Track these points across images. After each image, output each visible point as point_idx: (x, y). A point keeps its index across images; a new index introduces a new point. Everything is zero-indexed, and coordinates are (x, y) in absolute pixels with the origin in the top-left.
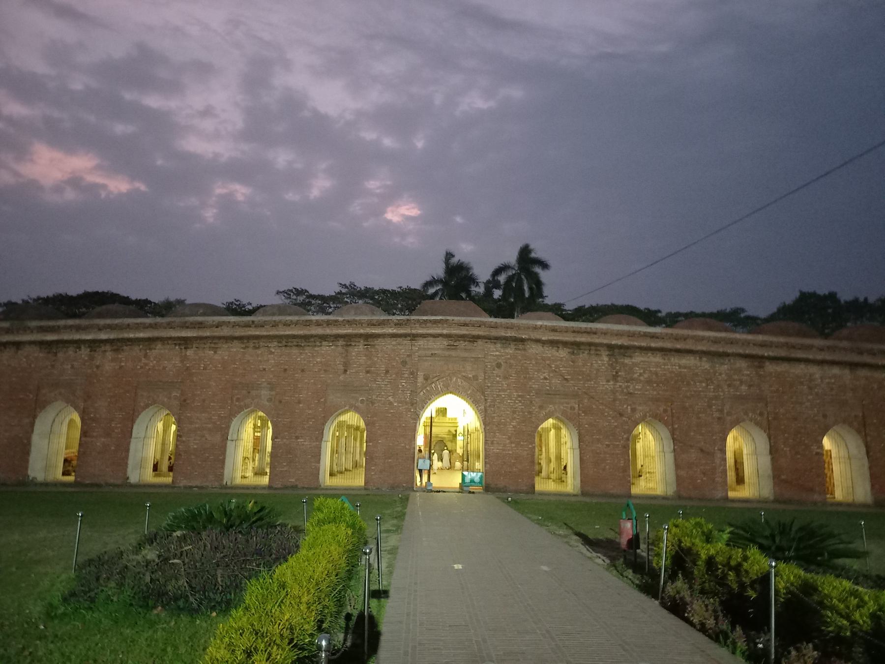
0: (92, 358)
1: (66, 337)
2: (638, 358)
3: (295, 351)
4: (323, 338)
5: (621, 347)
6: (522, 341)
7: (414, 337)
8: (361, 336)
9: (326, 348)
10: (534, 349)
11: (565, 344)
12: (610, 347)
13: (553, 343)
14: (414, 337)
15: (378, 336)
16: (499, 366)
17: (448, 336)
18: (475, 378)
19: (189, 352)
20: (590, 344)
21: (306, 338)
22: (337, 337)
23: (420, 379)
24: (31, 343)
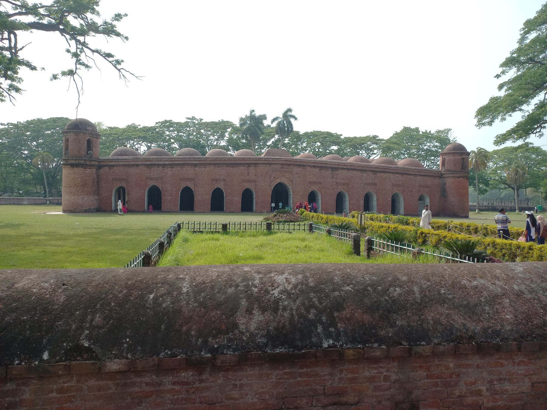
0: (164, 170)
1: (154, 163)
2: (340, 171)
3: (232, 168)
4: (241, 164)
5: (335, 168)
6: (305, 166)
7: (270, 164)
8: (253, 164)
9: (242, 168)
10: (308, 169)
11: (318, 167)
12: (332, 168)
13: (314, 167)
14: (270, 164)
15: (258, 164)
16: (297, 174)
17: (281, 164)
18: (290, 177)
19: (196, 168)
20: (326, 167)
21: (235, 164)
22: (246, 164)
23: (272, 178)
24: (142, 165)
